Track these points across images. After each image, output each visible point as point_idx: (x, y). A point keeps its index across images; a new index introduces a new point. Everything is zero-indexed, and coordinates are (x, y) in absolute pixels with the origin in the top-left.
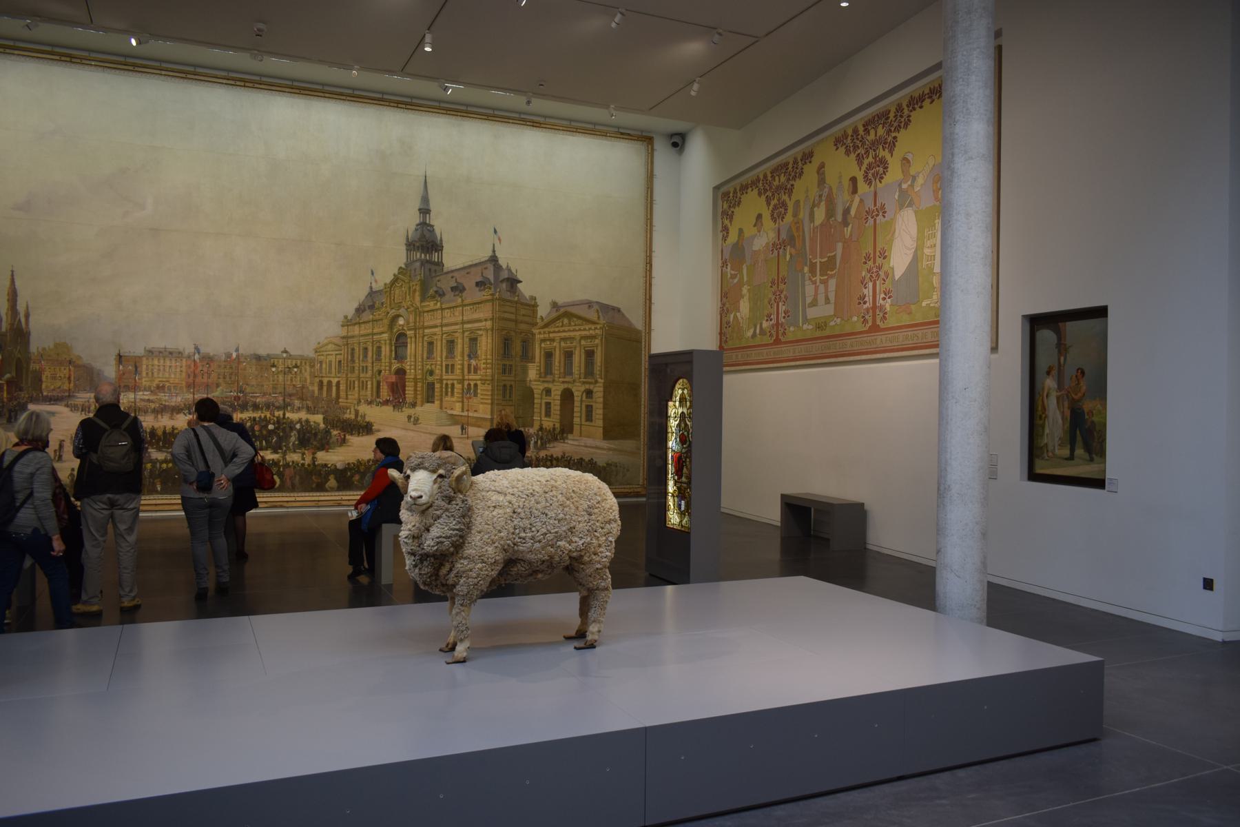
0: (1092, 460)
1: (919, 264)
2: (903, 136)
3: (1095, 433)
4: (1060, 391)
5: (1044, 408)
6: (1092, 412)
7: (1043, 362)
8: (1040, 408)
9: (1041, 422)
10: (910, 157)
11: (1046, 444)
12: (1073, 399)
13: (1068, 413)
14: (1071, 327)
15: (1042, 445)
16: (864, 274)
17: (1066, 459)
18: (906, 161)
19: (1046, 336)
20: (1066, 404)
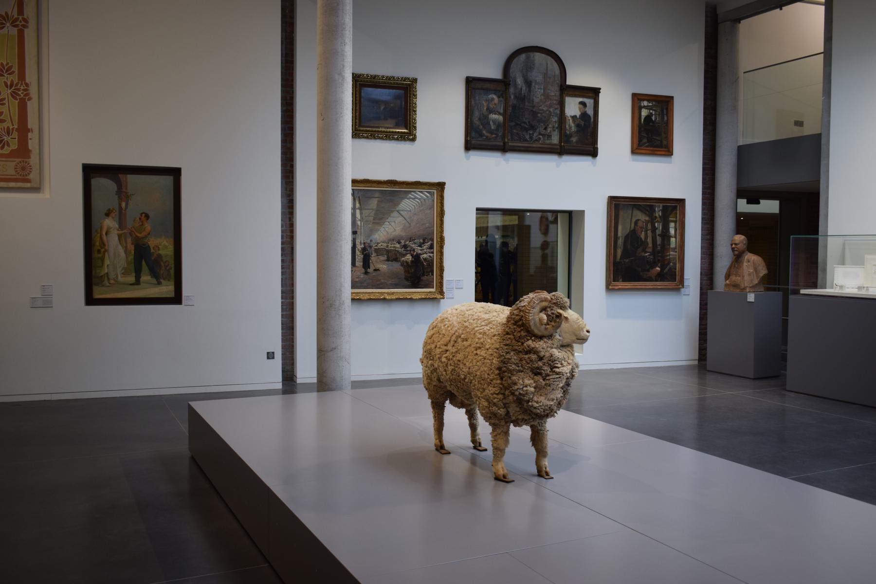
0: (159, 283)
3: (162, 263)
4: (122, 230)
5: (103, 245)
6: (158, 248)
7: (100, 203)
8: (98, 244)
9: (100, 255)
11: (107, 273)
12: (137, 236)
13: (131, 248)
14: (132, 179)
15: (102, 274)
17: (131, 284)
19: (103, 185)
20: (129, 240)
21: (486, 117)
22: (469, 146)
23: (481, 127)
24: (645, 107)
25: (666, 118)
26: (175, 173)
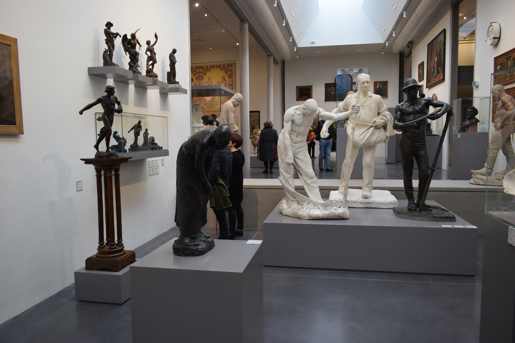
1: (214, 99)
2: (208, 73)
10: (211, 78)
16: (196, 99)
18: (209, 78)
21: (330, 93)
22: (326, 100)
23: (329, 95)
24: (378, 85)
25: (385, 87)
26: (259, 112)
